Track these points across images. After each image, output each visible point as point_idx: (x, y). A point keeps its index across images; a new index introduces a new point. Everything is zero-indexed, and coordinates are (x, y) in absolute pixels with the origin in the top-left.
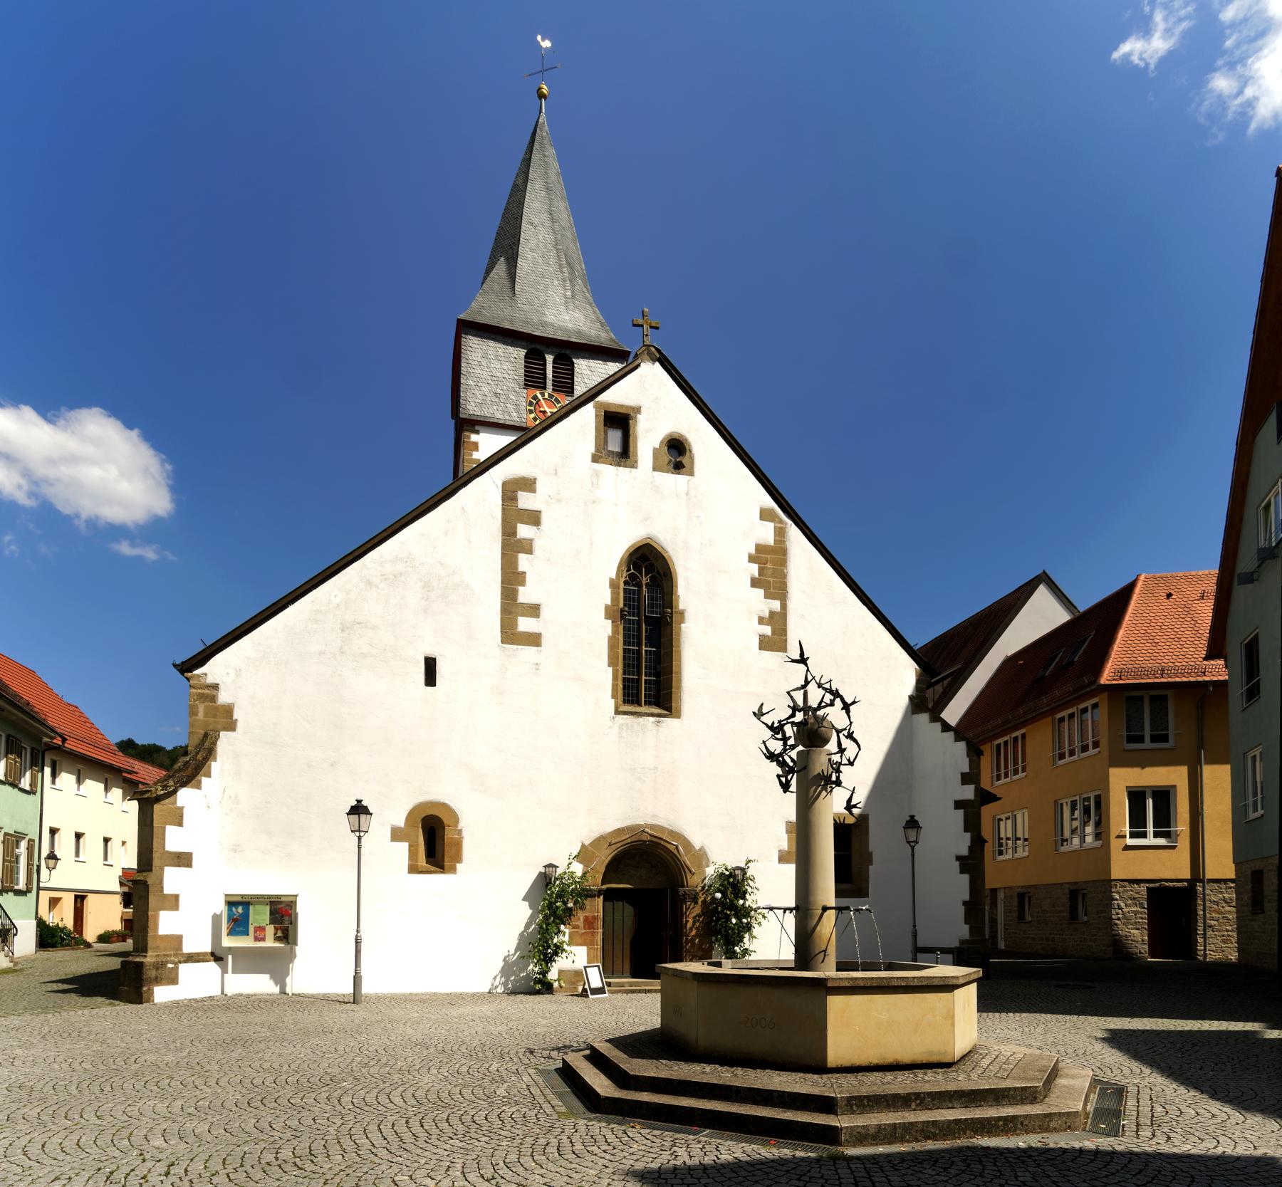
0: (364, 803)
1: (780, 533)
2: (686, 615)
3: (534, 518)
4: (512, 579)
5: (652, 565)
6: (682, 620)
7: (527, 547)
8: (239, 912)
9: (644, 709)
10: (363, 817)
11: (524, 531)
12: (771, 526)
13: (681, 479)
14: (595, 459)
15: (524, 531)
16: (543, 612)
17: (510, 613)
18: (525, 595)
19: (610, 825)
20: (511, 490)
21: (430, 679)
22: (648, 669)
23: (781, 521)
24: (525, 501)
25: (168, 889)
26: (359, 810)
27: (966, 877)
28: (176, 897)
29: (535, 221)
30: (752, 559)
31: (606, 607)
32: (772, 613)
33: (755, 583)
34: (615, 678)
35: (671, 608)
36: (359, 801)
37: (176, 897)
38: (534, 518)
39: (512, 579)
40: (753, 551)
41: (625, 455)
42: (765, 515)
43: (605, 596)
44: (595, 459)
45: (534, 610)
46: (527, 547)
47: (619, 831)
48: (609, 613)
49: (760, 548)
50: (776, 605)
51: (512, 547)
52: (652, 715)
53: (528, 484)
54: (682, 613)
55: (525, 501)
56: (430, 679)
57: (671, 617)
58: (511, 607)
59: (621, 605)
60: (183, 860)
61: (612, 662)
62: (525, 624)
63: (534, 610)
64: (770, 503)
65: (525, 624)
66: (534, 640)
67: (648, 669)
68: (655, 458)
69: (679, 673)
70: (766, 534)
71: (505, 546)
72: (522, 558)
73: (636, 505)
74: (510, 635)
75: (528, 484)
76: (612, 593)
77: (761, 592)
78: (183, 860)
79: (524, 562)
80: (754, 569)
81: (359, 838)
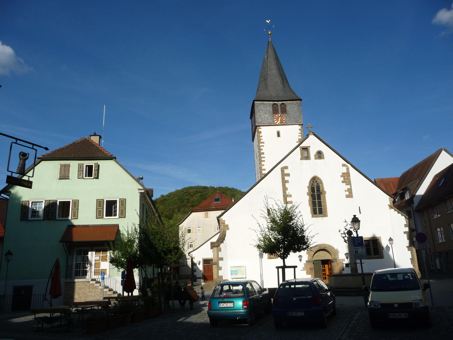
1: (348, 169)
3: (288, 175)
4: (285, 189)
7: (287, 182)
11: (286, 178)
12: (345, 168)
13: (322, 160)
14: (301, 159)
15: (286, 178)
16: (292, 196)
20: (283, 169)
24: (286, 171)
27: (410, 252)
30: (341, 176)
32: (348, 189)
33: (343, 182)
38: (288, 175)
39: (285, 189)
41: (308, 158)
42: (344, 165)
43: (307, 190)
44: (301, 159)
45: (290, 196)
46: (287, 182)
48: (308, 194)
49: (343, 174)
50: (349, 187)
51: (284, 182)
53: (286, 168)
54: (325, 192)
55: (286, 171)
61: (310, 206)
63: (290, 196)
64: (344, 162)
68: (315, 156)
70: (344, 170)
71: (283, 182)
72: (286, 184)
73: (312, 168)
75: (286, 168)
77: (345, 184)
79: (287, 185)
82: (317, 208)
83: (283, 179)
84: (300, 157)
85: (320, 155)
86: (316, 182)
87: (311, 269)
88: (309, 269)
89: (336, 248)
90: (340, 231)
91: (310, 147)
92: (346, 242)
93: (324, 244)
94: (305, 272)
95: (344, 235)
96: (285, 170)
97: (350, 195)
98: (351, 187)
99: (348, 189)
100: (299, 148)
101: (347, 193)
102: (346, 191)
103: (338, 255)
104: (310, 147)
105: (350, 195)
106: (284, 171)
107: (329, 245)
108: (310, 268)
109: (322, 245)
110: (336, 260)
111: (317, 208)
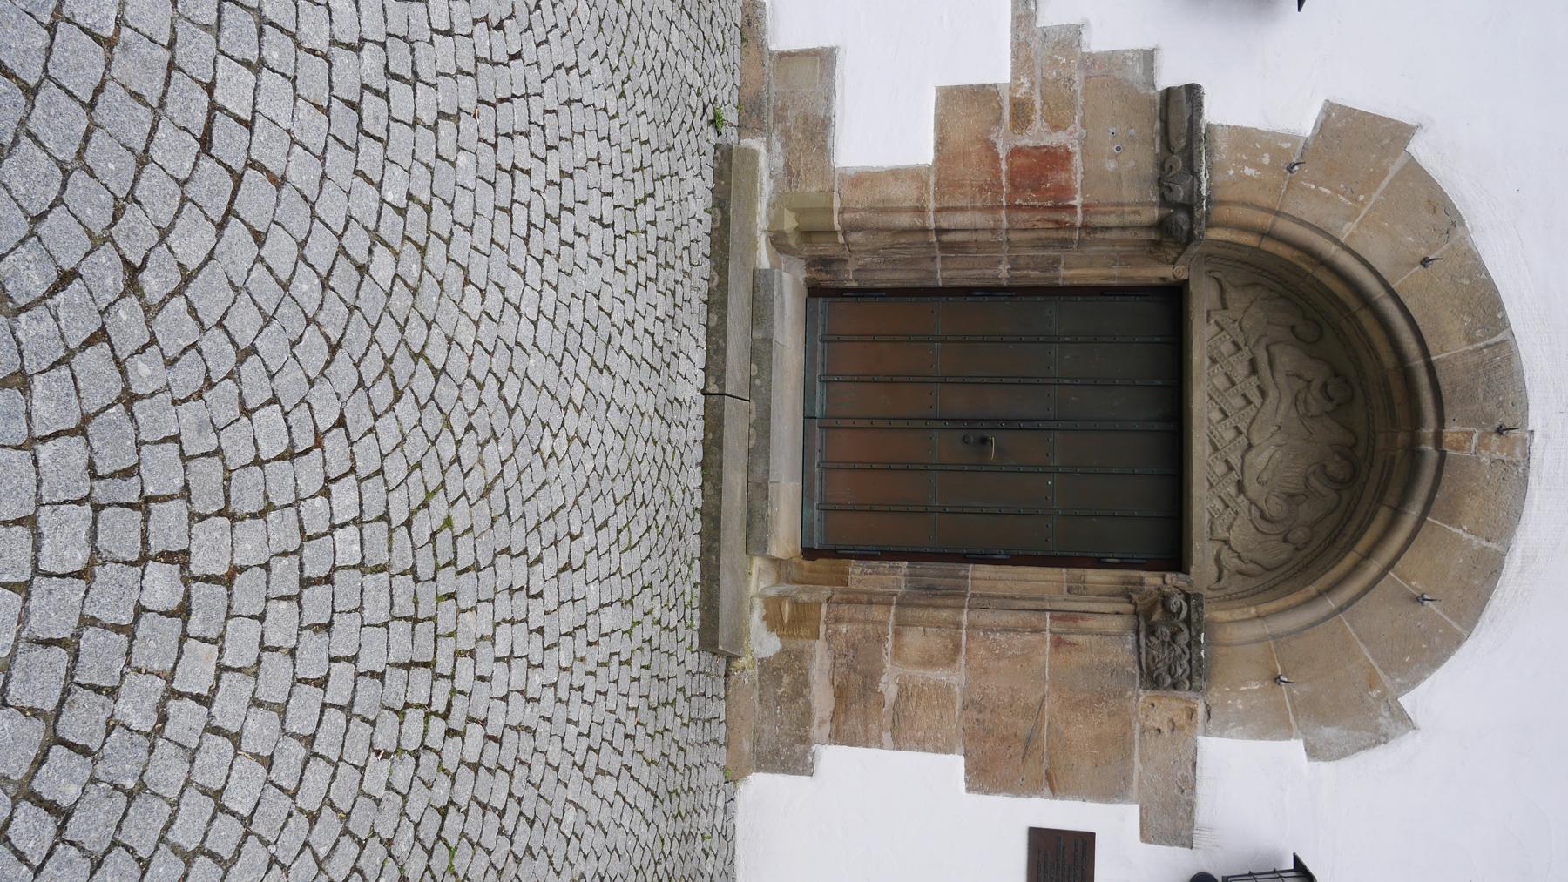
88: (1037, 135)
89: (1436, 697)
93: (1515, 474)
107: (1489, 569)
108: (1056, 158)
109: (1507, 428)
110: (1172, 654)
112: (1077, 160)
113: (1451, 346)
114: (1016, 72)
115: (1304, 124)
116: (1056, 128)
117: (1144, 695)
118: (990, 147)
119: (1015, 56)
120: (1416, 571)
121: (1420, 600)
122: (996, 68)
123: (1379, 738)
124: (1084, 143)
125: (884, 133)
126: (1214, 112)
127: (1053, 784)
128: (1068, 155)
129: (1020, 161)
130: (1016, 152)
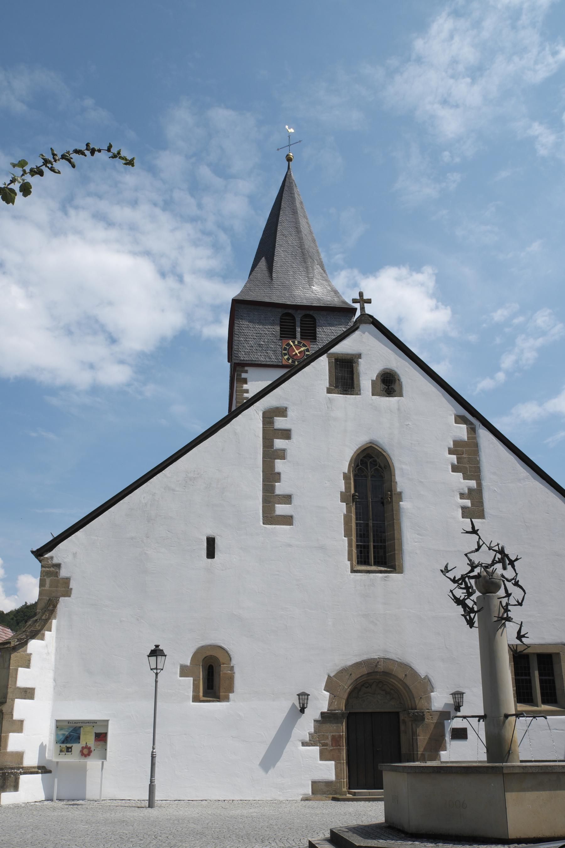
0: (160, 648)
2: (403, 495)
4: (270, 477)
5: (375, 461)
6: (401, 499)
8: (70, 735)
9: (374, 568)
10: (159, 658)
16: (295, 500)
17: (270, 502)
18: (280, 489)
19: (351, 661)
21: (211, 554)
22: (375, 540)
23: (471, 423)
25: (17, 716)
26: (156, 652)
28: (22, 722)
29: (285, 233)
30: (451, 452)
31: (341, 492)
33: (455, 469)
34: (350, 545)
35: (391, 491)
36: (157, 646)
37: (22, 722)
39: (270, 477)
40: (451, 445)
42: (460, 419)
45: (287, 499)
47: (358, 665)
48: (344, 498)
52: (381, 572)
54: (400, 494)
56: (211, 554)
57: (391, 498)
58: (270, 497)
59: (353, 491)
60: (28, 693)
61: (347, 534)
62: (281, 509)
63: (287, 499)
65: (281, 509)
66: (288, 520)
67: (375, 540)
69: (400, 539)
74: (270, 518)
76: (345, 483)
78: (28, 693)
80: (454, 458)
81: (157, 674)
82: (372, 544)
83: (268, 443)
84: (325, 382)
85: (388, 384)
86: (374, 463)
87: (336, 740)
88: (329, 741)
90: (445, 571)
91: (359, 356)
92: (471, 623)
94: (315, 750)
95: (460, 593)
96: (276, 418)
97: (475, 507)
98: (479, 484)
99: (470, 490)
100: (324, 360)
101: (467, 503)
102: (462, 496)
103: (429, 699)
104: (359, 356)
105: (475, 507)
106: (272, 423)
108: (333, 738)
111: (372, 544)
112: (334, 734)
113: (365, 671)
114: (317, 746)
115: (327, 694)
116: (328, 738)
117: (426, 720)
118: (331, 750)
119: (314, 746)
120: (401, 676)
121: (406, 675)
122: (316, 749)
123: (429, 680)
124: (331, 732)
125: (328, 771)
126: (325, 710)
127: (443, 736)
128: (333, 735)
129: (334, 744)
130: (332, 745)
